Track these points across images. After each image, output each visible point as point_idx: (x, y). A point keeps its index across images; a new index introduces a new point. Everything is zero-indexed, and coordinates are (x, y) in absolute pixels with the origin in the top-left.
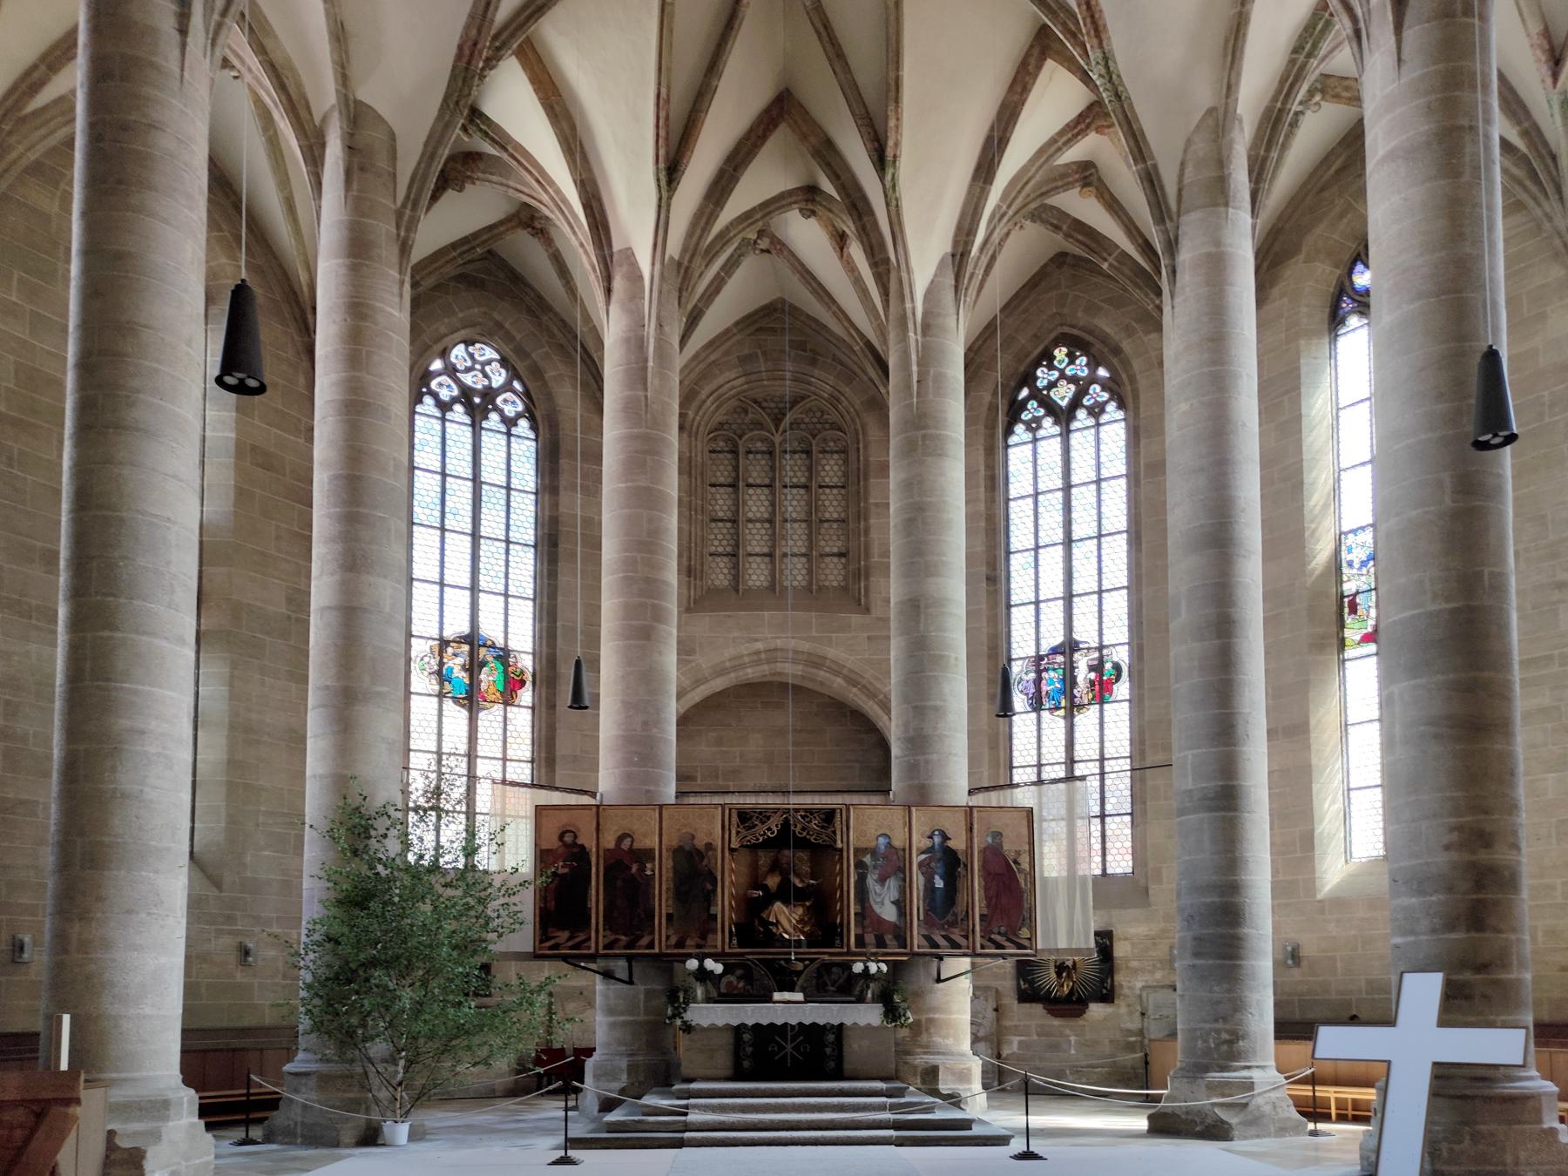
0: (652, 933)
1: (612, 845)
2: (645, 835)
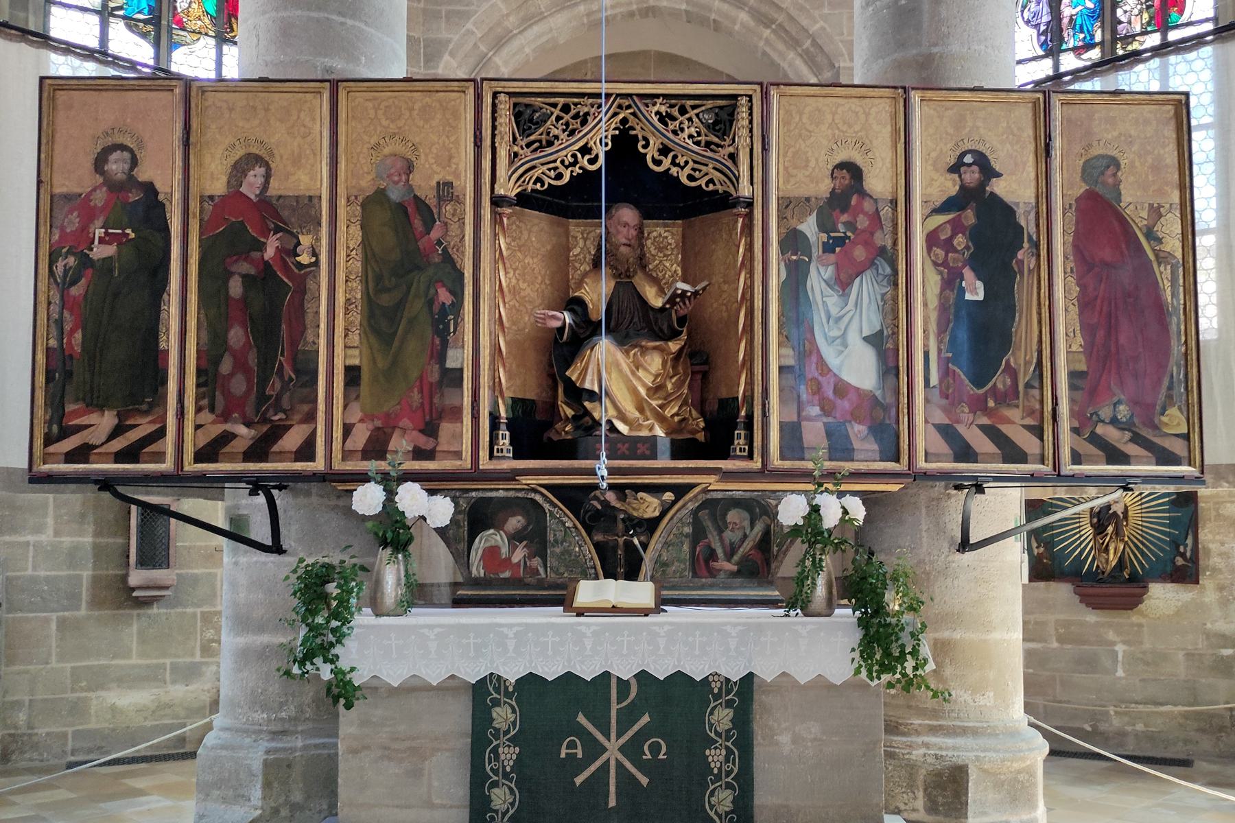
0: (311, 417)
1: (219, 187)
2: (297, 161)
